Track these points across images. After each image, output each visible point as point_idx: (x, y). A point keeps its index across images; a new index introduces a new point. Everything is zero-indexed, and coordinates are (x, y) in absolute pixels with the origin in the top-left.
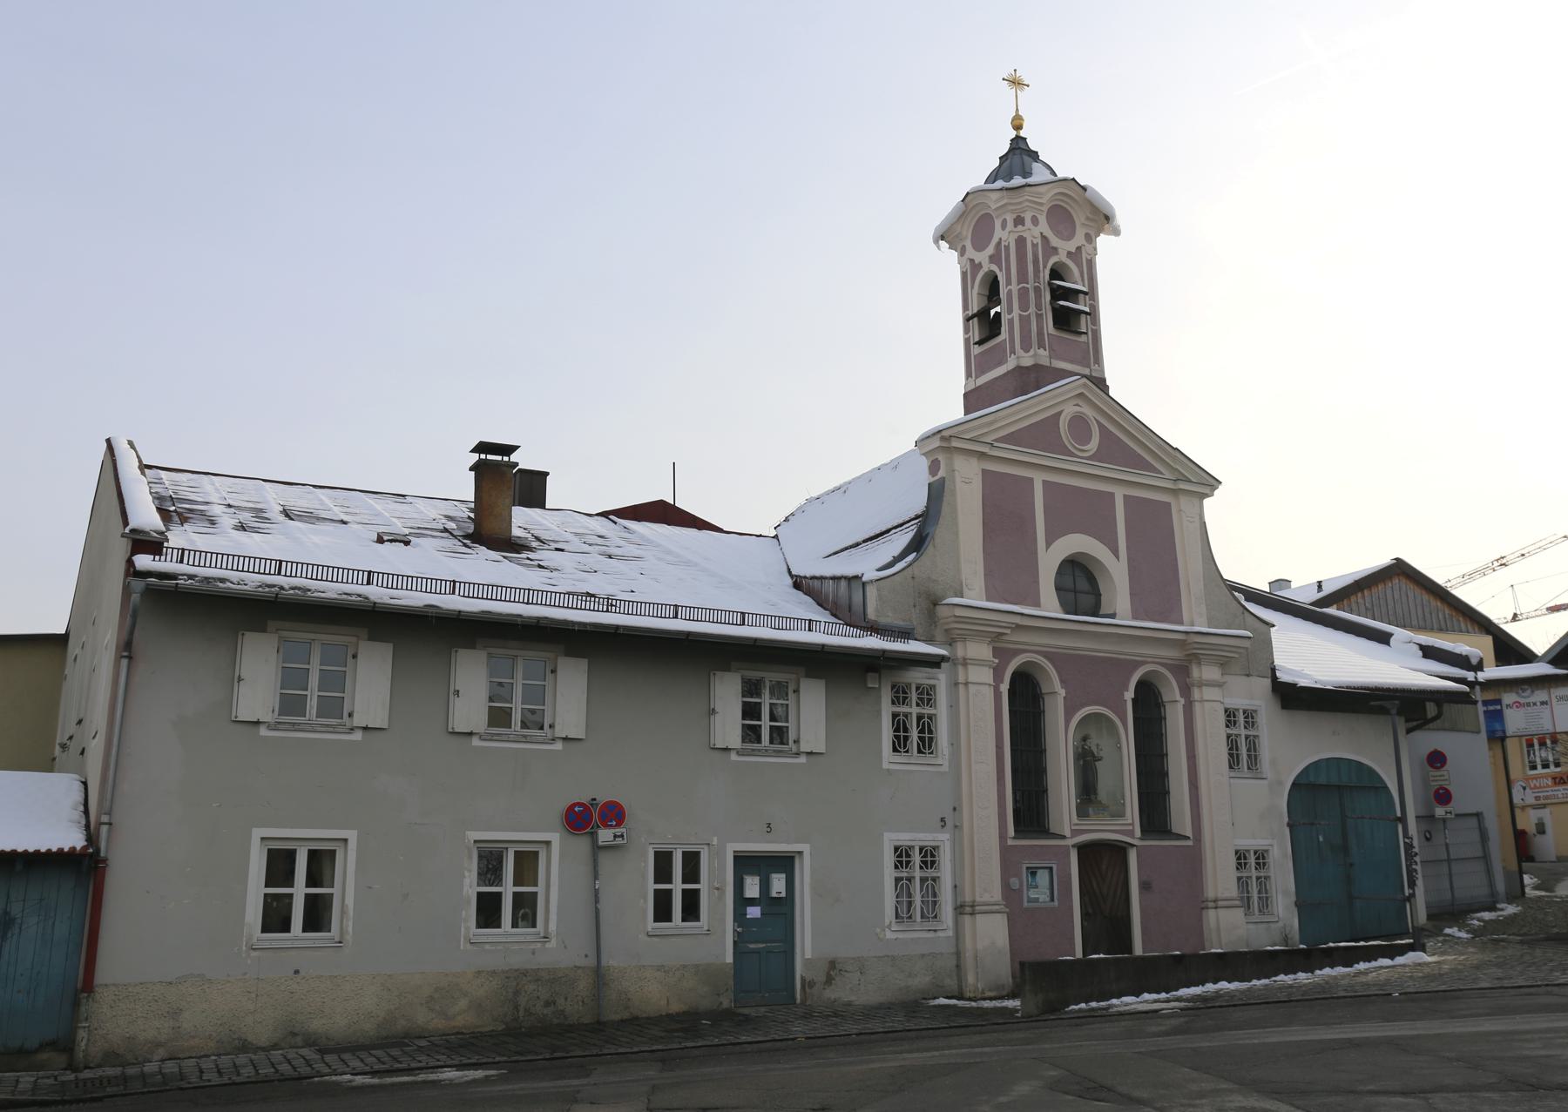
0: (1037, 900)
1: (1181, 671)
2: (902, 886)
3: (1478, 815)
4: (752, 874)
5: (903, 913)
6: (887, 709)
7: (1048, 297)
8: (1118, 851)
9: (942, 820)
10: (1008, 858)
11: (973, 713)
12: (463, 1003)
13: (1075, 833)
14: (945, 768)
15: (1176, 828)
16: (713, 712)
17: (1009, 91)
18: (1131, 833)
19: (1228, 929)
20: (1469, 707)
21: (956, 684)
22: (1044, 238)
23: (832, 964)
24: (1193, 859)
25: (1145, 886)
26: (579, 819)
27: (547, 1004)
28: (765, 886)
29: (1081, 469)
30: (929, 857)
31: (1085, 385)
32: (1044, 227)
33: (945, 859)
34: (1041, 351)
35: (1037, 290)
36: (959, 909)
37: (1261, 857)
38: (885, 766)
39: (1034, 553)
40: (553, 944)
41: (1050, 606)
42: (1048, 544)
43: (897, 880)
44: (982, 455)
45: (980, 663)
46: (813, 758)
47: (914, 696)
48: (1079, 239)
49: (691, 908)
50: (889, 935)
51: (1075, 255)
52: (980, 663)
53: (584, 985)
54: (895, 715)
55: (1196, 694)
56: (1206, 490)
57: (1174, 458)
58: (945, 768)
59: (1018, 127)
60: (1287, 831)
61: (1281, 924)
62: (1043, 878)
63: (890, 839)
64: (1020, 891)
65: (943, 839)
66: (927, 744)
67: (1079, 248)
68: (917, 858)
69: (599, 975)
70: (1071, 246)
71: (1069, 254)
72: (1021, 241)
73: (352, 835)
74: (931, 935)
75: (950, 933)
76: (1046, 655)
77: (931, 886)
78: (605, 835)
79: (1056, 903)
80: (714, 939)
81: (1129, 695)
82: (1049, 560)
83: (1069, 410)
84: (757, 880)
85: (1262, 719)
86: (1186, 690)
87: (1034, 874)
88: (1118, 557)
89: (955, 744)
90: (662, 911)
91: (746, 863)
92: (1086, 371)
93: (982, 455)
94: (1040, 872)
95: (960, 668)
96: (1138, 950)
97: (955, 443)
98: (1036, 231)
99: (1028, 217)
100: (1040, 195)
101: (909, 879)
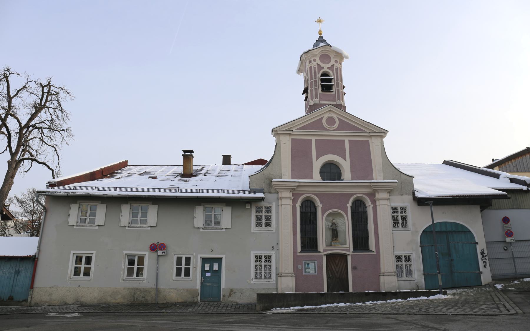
0: (309, 272)
1: (372, 196)
4: (208, 263)
5: (257, 275)
8: (344, 257)
9: (273, 247)
10: (297, 260)
12: (120, 296)
13: (324, 251)
14: (274, 231)
15: (370, 249)
16: (194, 217)
17: (318, 24)
18: (349, 251)
19: (388, 283)
23: (232, 290)
25: (354, 268)
26: (153, 248)
27: (143, 297)
28: (211, 267)
29: (331, 134)
30: (268, 259)
31: (331, 107)
32: (318, 61)
33: (273, 259)
35: (315, 81)
36: (278, 275)
37: (408, 258)
38: (252, 231)
40: (145, 281)
41: (317, 178)
42: (317, 159)
43: (256, 266)
44: (290, 134)
45: (286, 198)
46: (227, 230)
48: (333, 62)
49: (187, 273)
50: (252, 282)
52: (286, 198)
53: (153, 293)
54: (257, 216)
56: (382, 134)
57: (369, 126)
58: (274, 231)
59: (320, 34)
60: (420, 248)
61: (416, 281)
62: (312, 265)
64: (302, 269)
65: (273, 254)
66: (268, 224)
67: (333, 66)
68: (263, 259)
69: (158, 291)
71: (328, 68)
72: (311, 68)
73: (94, 252)
74: (267, 283)
75: (275, 282)
76: (315, 194)
78: (160, 252)
79: (316, 273)
80: (195, 281)
81: (349, 205)
82: (317, 164)
83: (326, 116)
84: (209, 265)
85: (408, 210)
86: (374, 202)
87: (308, 264)
90: (178, 273)
91: (205, 260)
92: (335, 103)
93: (290, 134)
96: (351, 290)
97: (279, 132)
98: (315, 63)
99: (312, 60)
100: (315, 52)
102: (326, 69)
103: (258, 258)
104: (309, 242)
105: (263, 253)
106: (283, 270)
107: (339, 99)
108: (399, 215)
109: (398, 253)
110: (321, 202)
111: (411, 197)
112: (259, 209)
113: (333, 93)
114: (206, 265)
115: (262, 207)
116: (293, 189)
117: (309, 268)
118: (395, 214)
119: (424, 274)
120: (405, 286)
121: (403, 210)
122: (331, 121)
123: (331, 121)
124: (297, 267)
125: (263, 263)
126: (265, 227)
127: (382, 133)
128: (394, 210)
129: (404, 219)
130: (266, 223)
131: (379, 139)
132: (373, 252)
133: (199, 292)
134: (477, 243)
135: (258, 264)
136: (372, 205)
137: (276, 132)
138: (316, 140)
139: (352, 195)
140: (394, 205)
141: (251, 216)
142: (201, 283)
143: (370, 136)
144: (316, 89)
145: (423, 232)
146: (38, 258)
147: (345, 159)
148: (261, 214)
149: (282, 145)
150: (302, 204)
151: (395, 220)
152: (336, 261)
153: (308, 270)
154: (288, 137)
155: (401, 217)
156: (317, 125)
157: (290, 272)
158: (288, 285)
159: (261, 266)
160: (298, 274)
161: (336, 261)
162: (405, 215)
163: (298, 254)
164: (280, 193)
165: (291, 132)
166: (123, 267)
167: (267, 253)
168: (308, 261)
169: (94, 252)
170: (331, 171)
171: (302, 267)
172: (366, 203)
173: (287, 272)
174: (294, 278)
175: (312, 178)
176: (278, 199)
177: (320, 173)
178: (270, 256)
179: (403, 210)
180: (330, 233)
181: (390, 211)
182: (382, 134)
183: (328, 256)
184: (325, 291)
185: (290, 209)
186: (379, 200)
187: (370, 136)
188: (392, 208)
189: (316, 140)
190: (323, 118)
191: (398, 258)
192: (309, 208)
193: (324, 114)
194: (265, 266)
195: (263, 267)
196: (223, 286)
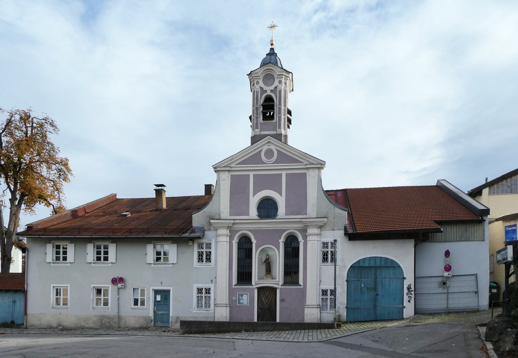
0: (243, 303)
1: (304, 231)
2: (199, 299)
3: (476, 275)
5: (199, 305)
6: (196, 250)
7: (261, 109)
8: (274, 290)
10: (231, 292)
11: (223, 250)
12: (91, 322)
13: (256, 284)
16: (146, 254)
18: (278, 284)
19: (311, 315)
20: (440, 234)
22: (261, 88)
24: (303, 293)
25: (282, 300)
26: (114, 281)
27: (108, 323)
29: (269, 167)
30: (208, 291)
32: (261, 84)
33: (212, 291)
37: (333, 292)
38: (195, 266)
42: (254, 195)
43: (198, 297)
44: (229, 171)
45: (223, 235)
47: (204, 246)
48: (276, 83)
49: (143, 303)
50: (194, 311)
51: (274, 91)
52: (223, 235)
53: (116, 320)
55: (309, 238)
57: (306, 157)
62: (245, 297)
63: (195, 286)
64: (236, 300)
65: (212, 286)
66: (209, 260)
67: (276, 87)
68: (204, 291)
69: (119, 317)
70: (272, 88)
71: (271, 91)
75: (213, 311)
76: (250, 231)
77: (208, 299)
78: (120, 285)
81: (282, 240)
82: (254, 201)
83: (265, 148)
85: (339, 245)
86: (305, 237)
87: (242, 296)
88: (281, 196)
89: (216, 259)
91: (156, 292)
92: (275, 132)
93: (229, 171)
94: (244, 295)
101: (327, 299)
102: (269, 93)
103: (200, 291)
104: (244, 276)
105: (204, 286)
106: (218, 302)
108: (329, 250)
109: (325, 287)
111: (342, 232)
112: (200, 246)
113: (274, 121)
114: (157, 296)
116: (229, 226)
118: (325, 250)
119: (347, 308)
120: (328, 317)
122: (269, 153)
123: (269, 153)
125: (204, 295)
127: (320, 165)
128: (325, 245)
129: (333, 254)
131: (317, 171)
133: (153, 318)
134: (405, 278)
135: (199, 295)
136: (303, 241)
139: (285, 230)
140: (325, 240)
142: (154, 312)
143: (308, 168)
144: (257, 118)
145: (351, 267)
146: (27, 291)
147: (281, 194)
148: (202, 250)
150: (240, 240)
151: (324, 256)
152: (267, 294)
153: (241, 301)
154: (227, 173)
157: (225, 303)
158: (222, 314)
159: (202, 297)
160: (232, 305)
161: (267, 294)
163: (234, 287)
165: (229, 169)
166: (92, 298)
167: (207, 286)
169: (69, 285)
170: (267, 208)
171: (236, 299)
172: (299, 238)
173: (222, 302)
174: (228, 308)
175: (248, 215)
176: (217, 236)
177: (258, 209)
180: (264, 268)
181: (320, 245)
182: (319, 166)
183: (260, 289)
184: (256, 320)
185: (226, 246)
186: (309, 235)
187: (308, 168)
188: (323, 243)
190: (261, 151)
191: (324, 292)
192: (247, 244)
193: (263, 146)
194: (205, 297)
195: (204, 298)
196: (171, 315)
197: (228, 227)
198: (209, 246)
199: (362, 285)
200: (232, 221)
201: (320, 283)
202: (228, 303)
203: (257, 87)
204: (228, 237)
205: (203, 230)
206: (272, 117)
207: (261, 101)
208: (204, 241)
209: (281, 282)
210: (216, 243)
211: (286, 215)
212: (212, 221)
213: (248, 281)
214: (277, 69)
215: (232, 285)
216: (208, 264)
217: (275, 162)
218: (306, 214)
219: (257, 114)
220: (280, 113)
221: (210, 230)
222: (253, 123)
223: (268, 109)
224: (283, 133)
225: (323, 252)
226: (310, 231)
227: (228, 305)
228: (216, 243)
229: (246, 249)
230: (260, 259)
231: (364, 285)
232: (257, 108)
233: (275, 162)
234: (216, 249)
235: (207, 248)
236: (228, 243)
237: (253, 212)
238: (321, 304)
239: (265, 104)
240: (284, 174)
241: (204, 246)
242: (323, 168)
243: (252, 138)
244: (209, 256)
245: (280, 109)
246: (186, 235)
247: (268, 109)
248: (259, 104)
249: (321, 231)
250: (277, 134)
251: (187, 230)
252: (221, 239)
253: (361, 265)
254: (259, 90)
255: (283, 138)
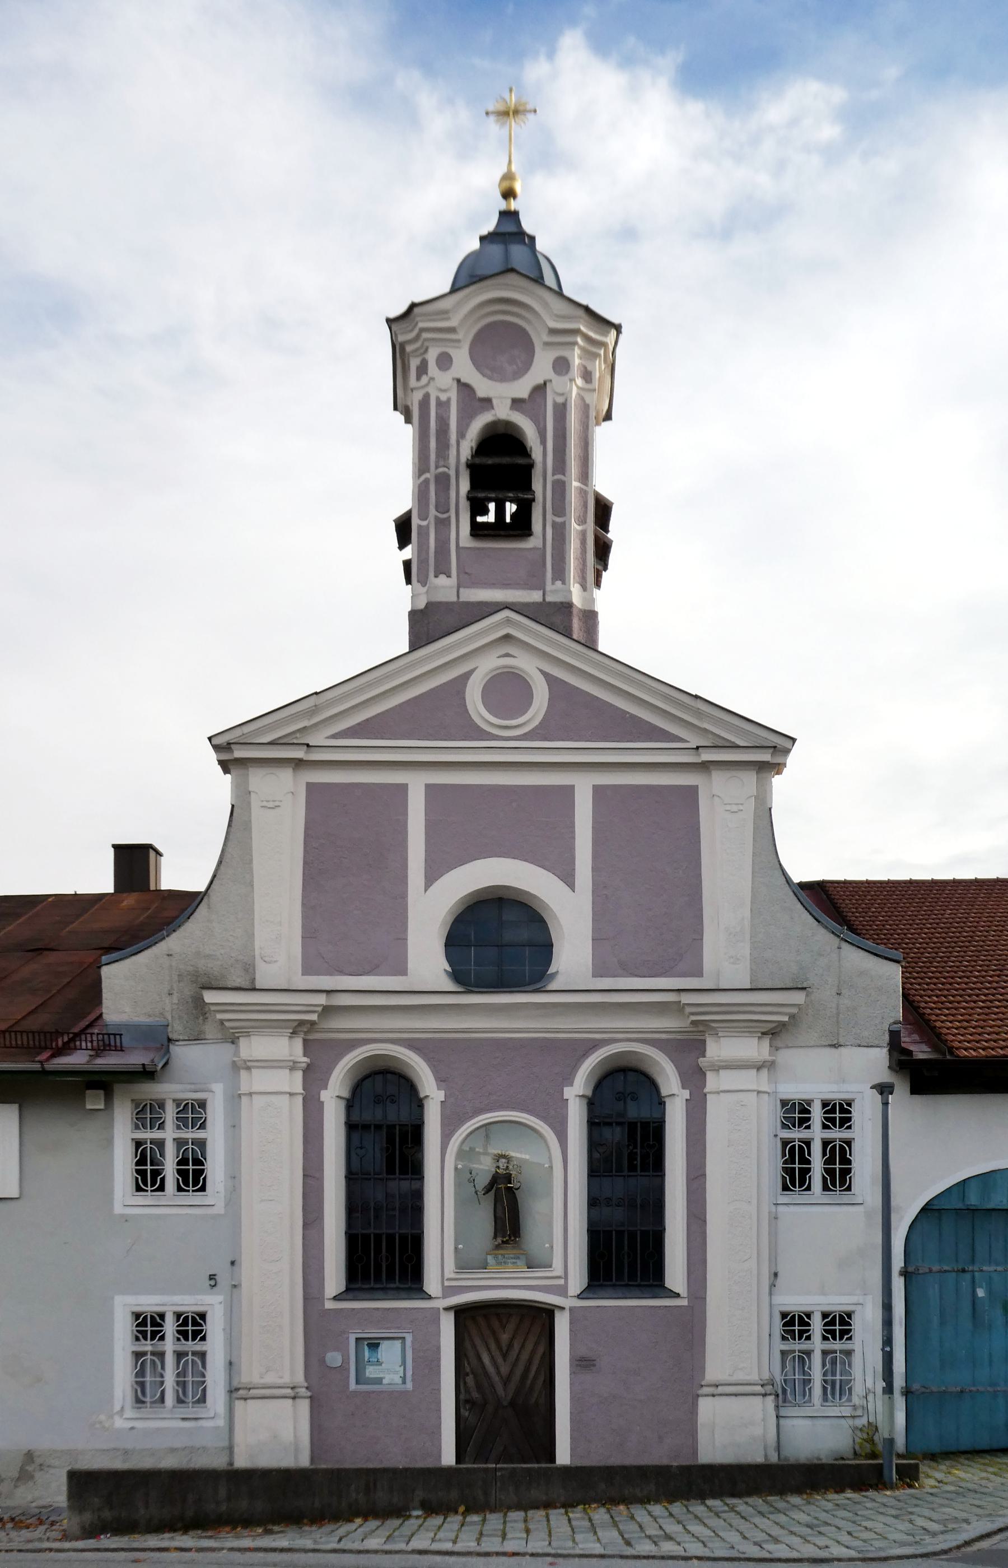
0: (379, 1381)
1: (689, 1049)
5: (145, 1394)
7: (465, 486)
8: (538, 1318)
9: (212, 1277)
10: (318, 1328)
14: (220, 1209)
15: (668, 1284)
18: (562, 1291)
21: (240, 1096)
23: (29, 1456)
24: (690, 1327)
25: (581, 1364)
29: (507, 753)
30: (192, 1326)
31: (508, 621)
32: (463, 367)
33: (215, 1327)
34: (442, 580)
36: (232, 1391)
37: (839, 1325)
38: (118, 1209)
39: (401, 898)
43: (138, 1355)
44: (298, 764)
47: (170, 1114)
50: (119, 1423)
55: (712, 1082)
57: (698, 713)
62: (390, 1353)
64: (344, 1368)
65: (213, 1305)
67: (540, 389)
68: (170, 1327)
71: (517, 403)
75: (221, 1422)
76: (412, 1045)
77: (193, 1367)
79: (409, 1386)
82: (430, 909)
83: (488, 665)
86: (694, 1078)
87: (374, 1346)
88: (572, 886)
89: (234, 1177)
92: (536, 596)
93: (298, 764)
94: (384, 1345)
95: (243, 1074)
96: (563, 1456)
99: (432, 356)
103: (148, 1325)
106: (251, 1374)
107: (560, 574)
109: (794, 1302)
110: (441, 1080)
111: (880, 1056)
112: (148, 1114)
113: (533, 542)
115: (162, 1105)
117: (379, 1363)
118: (797, 1134)
121: (839, 1113)
122: (508, 691)
123: (508, 691)
124: (322, 1361)
125: (169, 1345)
126: (180, 1189)
128: (796, 1113)
130: (183, 1173)
131: (750, 778)
132: (678, 1295)
135: (147, 1346)
136: (686, 1094)
137: (232, 751)
138: (428, 787)
139: (595, 1045)
140: (794, 1090)
141: (110, 1142)
143: (705, 767)
144: (442, 524)
145: (925, 1210)
147: (569, 879)
148: (157, 1135)
149: (258, 816)
152: (504, 1338)
153: (371, 1372)
154: (286, 776)
155: (825, 1143)
156: (436, 713)
157: (287, 1379)
158: (274, 1434)
159: (161, 1355)
162: (845, 1134)
163: (329, 1305)
164: (243, 1042)
165: (299, 754)
167: (189, 1303)
168: (372, 1333)
170: (499, 942)
171: (346, 1360)
172: (660, 1081)
173: (270, 1379)
175: (401, 970)
176: (240, 1066)
177: (446, 945)
178: (203, 1316)
179: (839, 1113)
181: (770, 1116)
182: (766, 757)
183: (463, 1314)
184: (448, 1457)
185: (290, 1116)
187: (705, 767)
188: (784, 1103)
189: (428, 787)
191: (795, 1324)
193: (475, 657)
194: (179, 1355)
195: (170, 1359)
197: (301, 1028)
198: (193, 1113)
199: (981, 1293)
200: (321, 1000)
201: (773, 1285)
202: (300, 1378)
203: (441, 384)
204: (299, 1075)
205: (160, 1040)
206: (521, 526)
207: (467, 449)
208: (168, 1091)
209: (577, 1278)
210: (235, 1099)
211: (599, 972)
212: (210, 997)
213: (403, 1278)
214: (546, 305)
215: (321, 1298)
216: (192, 1198)
217: (542, 732)
218: (699, 973)
219: (443, 506)
220: (560, 507)
221: (197, 1038)
222: (422, 550)
223: (501, 489)
224: (577, 597)
225: (785, 1143)
226: (717, 1049)
227: (303, 1391)
228: (235, 1099)
229: (391, 1128)
230: (465, 1177)
231: (990, 1292)
232: (443, 481)
233: (542, 732)
234: (234, 1126)
235: (182, 1122)
236: (299, 1100)
237: (427, 961)
238: (778, 1378)
239: (477, 461)
240: (584, 789)
241: (170, 1114)
242: (777, 768)
243: (415, 617)
244: (197, 1162)
245: (560, 489)
246: (77, 1059)
247: (501, 489)
248: (452, 461)
249: (775, 1048)
250: (544, 604)
251: (77, 1036)
252: (258, 1080)
253: (973, 1199)
254: (453, 395)
255: (576, 624)
